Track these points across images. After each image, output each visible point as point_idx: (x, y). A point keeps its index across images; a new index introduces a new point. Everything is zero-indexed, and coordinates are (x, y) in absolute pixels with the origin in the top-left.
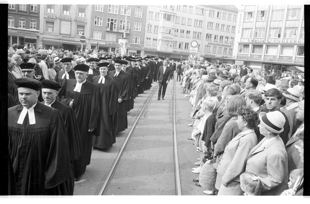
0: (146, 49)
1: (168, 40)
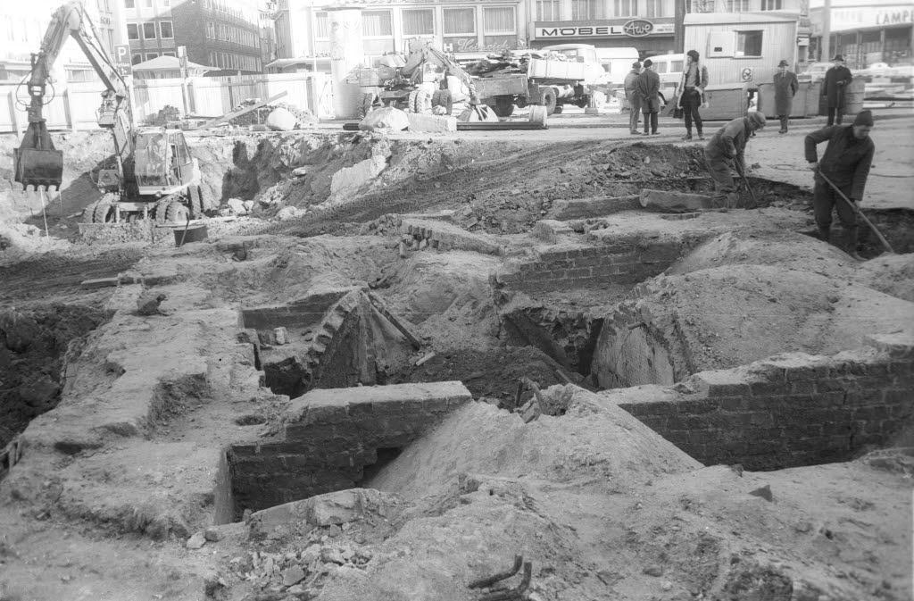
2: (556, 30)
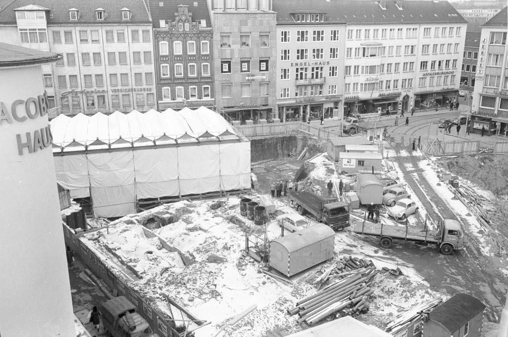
1: (374, 82)
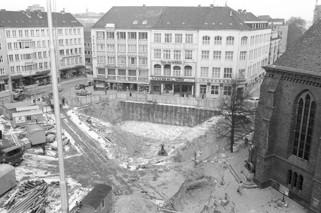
0: (13, 77)
1: (31, 64)
2: (156, 78)
